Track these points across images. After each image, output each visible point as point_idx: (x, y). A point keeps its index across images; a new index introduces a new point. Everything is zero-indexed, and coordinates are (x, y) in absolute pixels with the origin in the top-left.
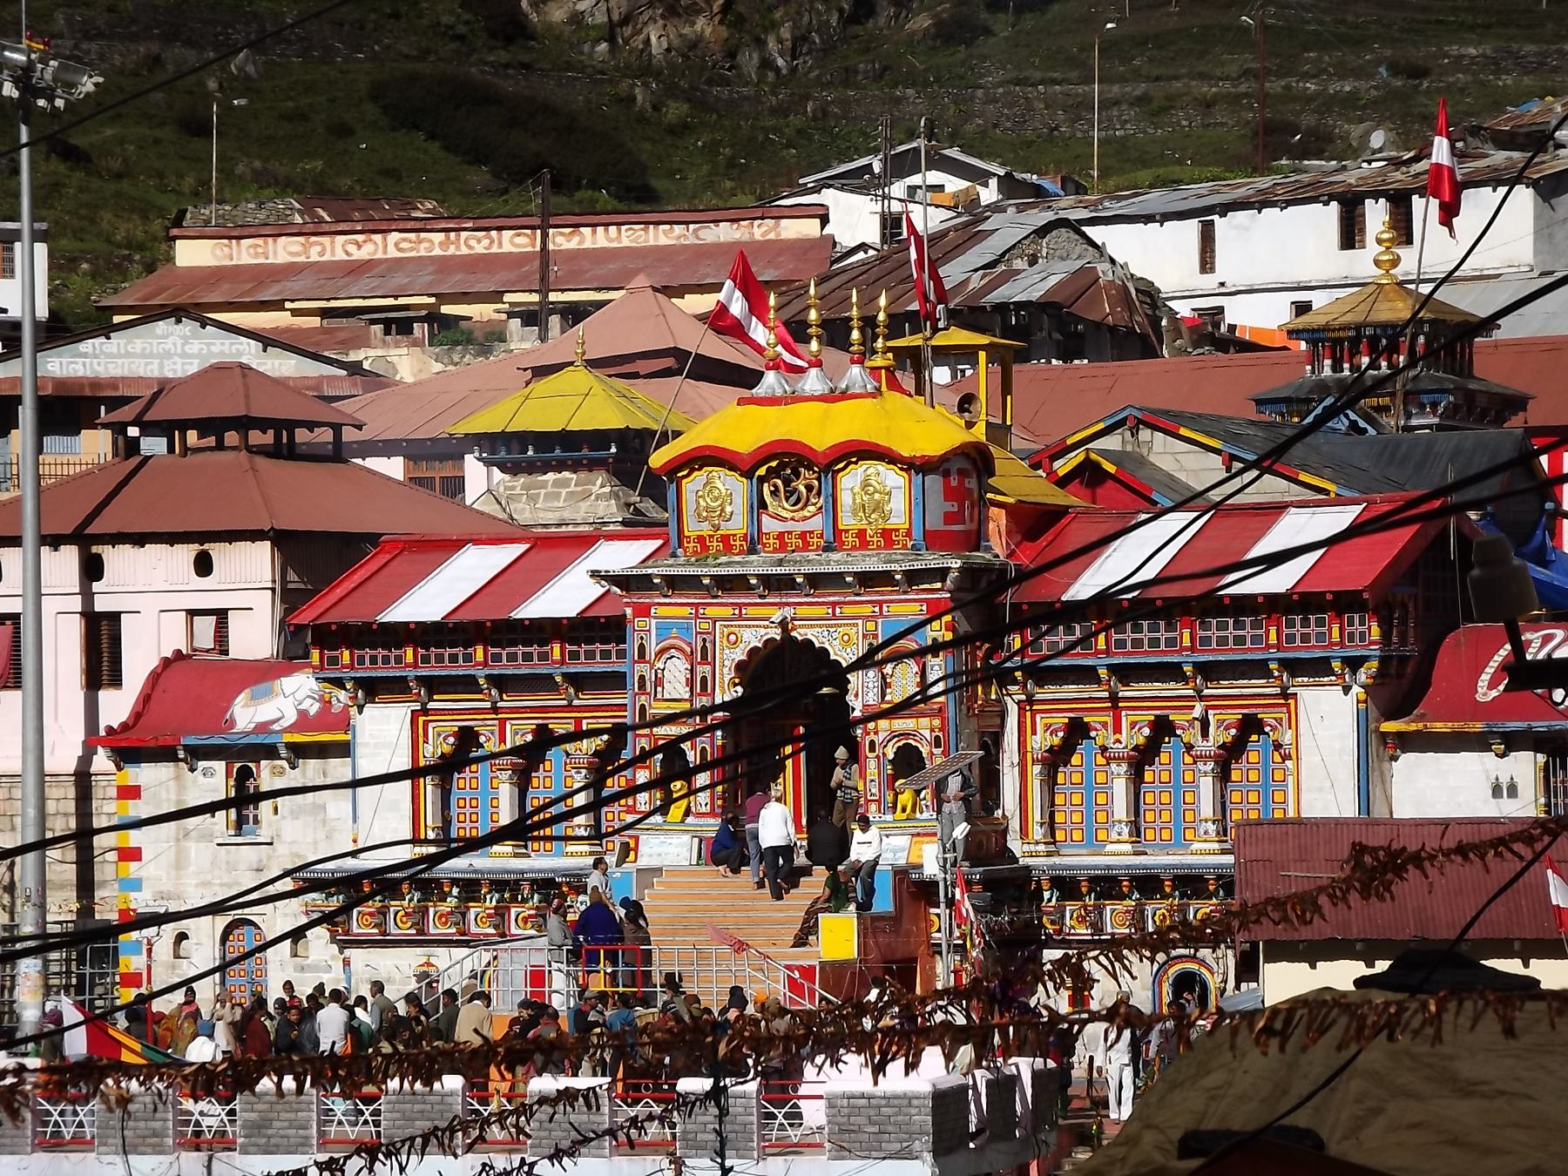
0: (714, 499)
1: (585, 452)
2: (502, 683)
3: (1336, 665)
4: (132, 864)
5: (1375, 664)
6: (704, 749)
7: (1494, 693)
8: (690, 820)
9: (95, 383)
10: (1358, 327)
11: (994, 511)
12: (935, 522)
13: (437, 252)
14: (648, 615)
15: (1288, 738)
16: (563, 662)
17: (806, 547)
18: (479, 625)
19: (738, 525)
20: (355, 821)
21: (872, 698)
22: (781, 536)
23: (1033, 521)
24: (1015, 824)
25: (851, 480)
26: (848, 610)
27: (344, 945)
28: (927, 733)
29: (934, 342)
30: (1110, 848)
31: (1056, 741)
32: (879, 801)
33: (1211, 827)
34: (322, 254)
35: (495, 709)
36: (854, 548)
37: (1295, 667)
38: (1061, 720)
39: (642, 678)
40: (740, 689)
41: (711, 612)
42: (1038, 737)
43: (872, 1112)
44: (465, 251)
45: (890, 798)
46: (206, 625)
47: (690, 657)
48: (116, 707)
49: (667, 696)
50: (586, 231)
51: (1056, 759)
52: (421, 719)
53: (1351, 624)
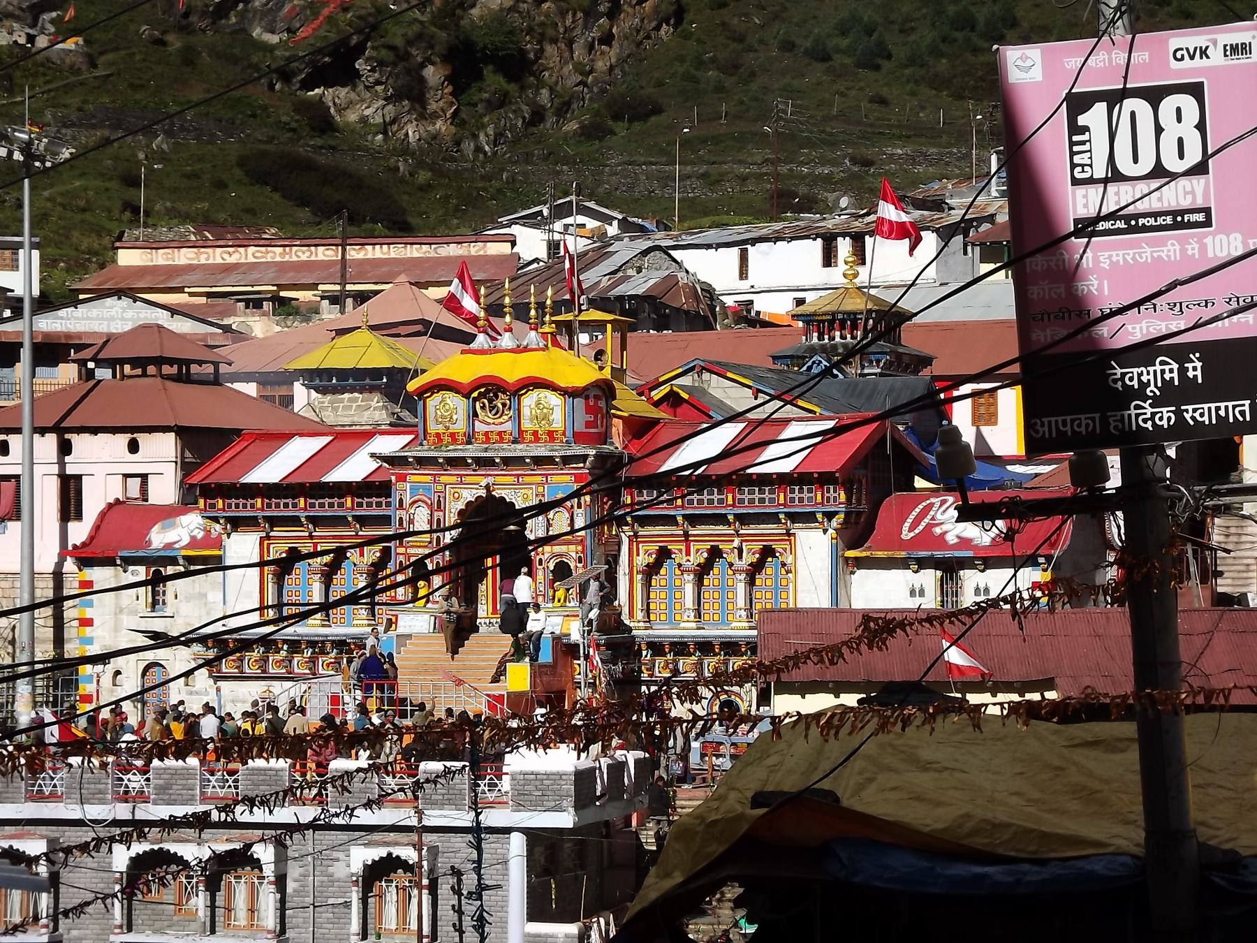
0: (447, 411)
1: (368, 381)
2: (316, 521)
3: (819, 516)
4: (88, 628)
5: (842, 516)
7: (912, 534)
8: (429, 605)
9: (68, 335)
10: (833, 314)
11: (615, 420)
12: (580, 427)
13: (278, 259)
15: (789, 560)
16: (353, 509)
17: (501, 440)
18: (302, 485)
19: (460, 427)
22: (486, 434)
23: (639, 427)
24: (626, 610)
25: (529, 400)
26: (527, 479)
27: (217, 679)
28: (573, 555)
29: (580, 318)
30: (683, 625)
31: (651, 560)
33: (744, 613)
34: (208, 259)
35: (311, 537)
36: (531, 442)
37: (794, 517)
39: (401, 519)
41: (443, 479)
42: (640, 558)
43: (538, 783)
44: (295, 258)
45: (551, 593)
46: (135, 484)
47: (430, 506)
48: (79, 532)
50: (369, 248)
51: (651, 571)
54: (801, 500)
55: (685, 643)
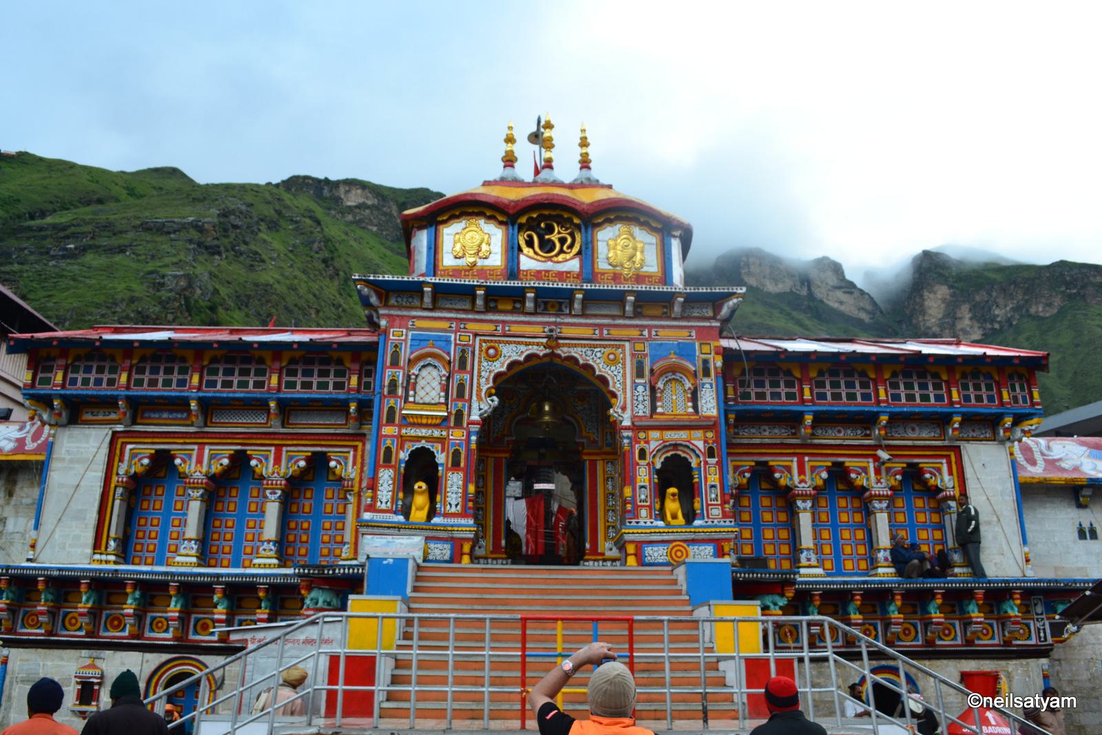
6: (456, 454)
8: (436, 520)
14: (407, 328)
15: (946, 480)
19: (496, 260)
20: (36, 527)
21: (643, 410)
22: (539, 272)
26: (615, 333)
28: (700, 444)
32: (650, 507)
38: (748, 463)
39: (393, 384)
40: (495, 398)
49: (418, 399)
52: (120, 441)
53: (1014, 389)
54: (979, 399)
55: (850, 591)
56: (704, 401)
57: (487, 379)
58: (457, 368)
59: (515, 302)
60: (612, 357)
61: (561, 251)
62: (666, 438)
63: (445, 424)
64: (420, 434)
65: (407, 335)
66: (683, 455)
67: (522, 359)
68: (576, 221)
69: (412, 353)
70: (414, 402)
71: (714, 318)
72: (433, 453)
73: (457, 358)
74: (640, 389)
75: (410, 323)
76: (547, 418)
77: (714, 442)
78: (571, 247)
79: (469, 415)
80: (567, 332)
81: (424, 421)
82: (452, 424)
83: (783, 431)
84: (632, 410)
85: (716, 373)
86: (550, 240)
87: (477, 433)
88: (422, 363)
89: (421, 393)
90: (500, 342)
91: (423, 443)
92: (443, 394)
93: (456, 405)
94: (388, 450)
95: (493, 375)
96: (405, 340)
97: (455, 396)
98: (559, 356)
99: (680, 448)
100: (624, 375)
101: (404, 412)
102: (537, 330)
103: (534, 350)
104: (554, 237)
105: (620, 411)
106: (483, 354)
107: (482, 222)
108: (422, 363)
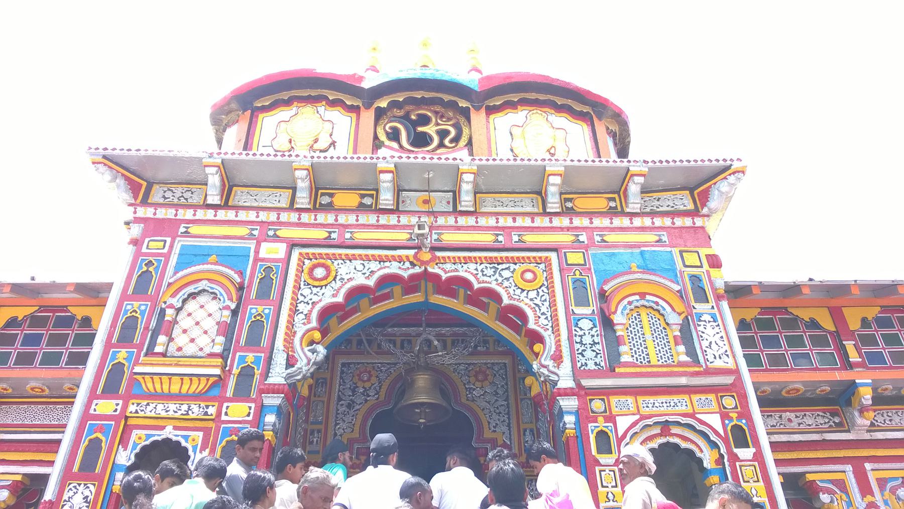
28: (715, 421)
39: (130, 325)
56: (705, 344)
57: (308, 316)
58: (253, 294)
59: (363, 196)
60: (529, 276)
61: (441, 145)
62: (645, 411)
63: (215, 392)
64: (163, 414)
65: (171, 246)
66: (684, 445)
67: (371, 283)
68: (463, 104)
69: (175, 273)
70: (164, 355)
71: (694, 213)
72: (186, 449)
73: (256, 282)
74: (585, 324)
75: (182, 230)
76: (423, 399)
77: (740, 417)
78: (456, 140)
79: (266, 374)
80: (449, 238)
81: (175, 389)
82: (229, 393)
83: (820, 420)
84: (574, 362)
85: (718, 298)
86: (425, 134)
87: (279, 411)
88: (191, 289)
89: (181, 340)
90: (334, 257)
91: (169, 432)
92: (221, 339)
93: (243, 358)
94: (95, 445)
95: (318, 308)
96: (167, 256)
97: (243, 342)
98: (438, 276)
99: (675, 430)
100: (553, 304)
101: (138, 369)
102: (401, 236)
103: (393, 268)
104: (430, 129)
105: (550, 363)
106: (305, 276)
107: (321, 109)
108: (191, 289)
